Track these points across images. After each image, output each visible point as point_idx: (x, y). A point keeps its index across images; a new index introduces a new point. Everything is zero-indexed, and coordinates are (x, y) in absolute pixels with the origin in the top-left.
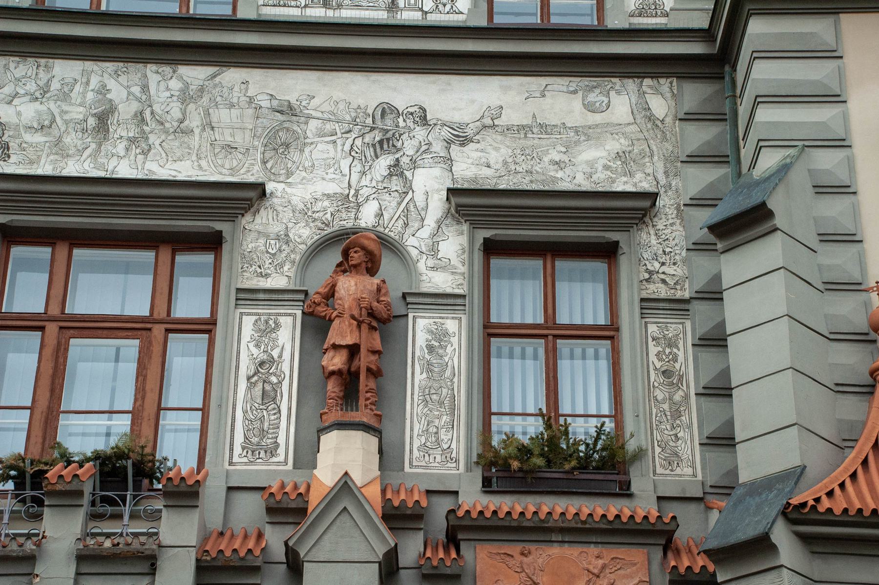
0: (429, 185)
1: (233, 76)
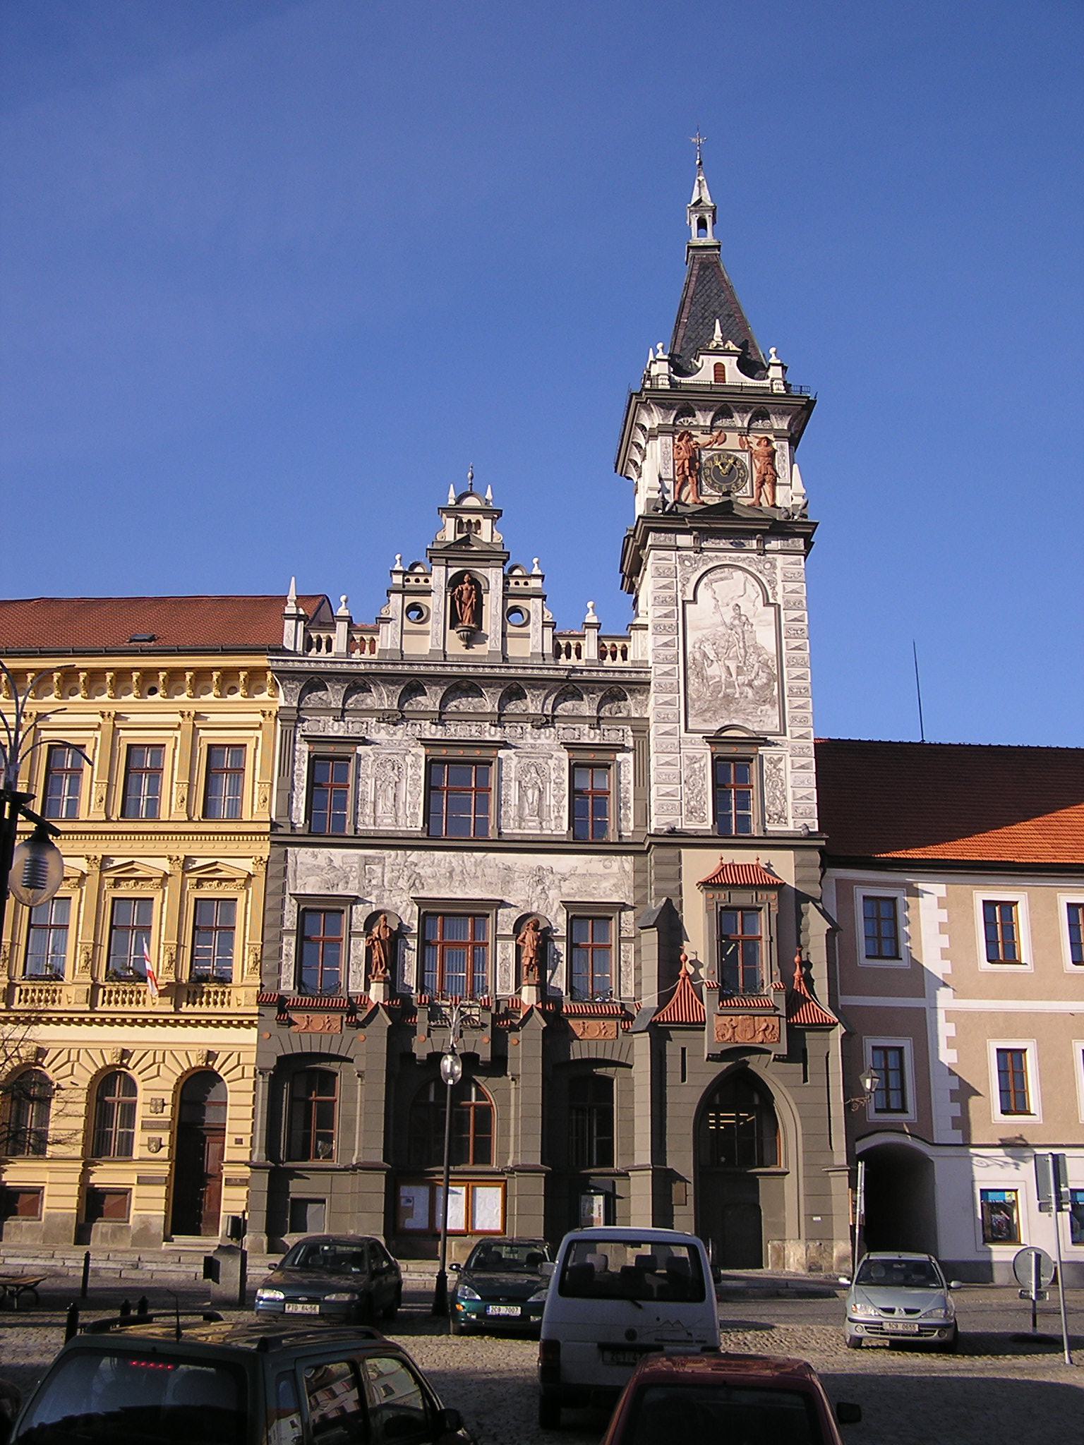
0: (555, 897)
1: (491, 855)
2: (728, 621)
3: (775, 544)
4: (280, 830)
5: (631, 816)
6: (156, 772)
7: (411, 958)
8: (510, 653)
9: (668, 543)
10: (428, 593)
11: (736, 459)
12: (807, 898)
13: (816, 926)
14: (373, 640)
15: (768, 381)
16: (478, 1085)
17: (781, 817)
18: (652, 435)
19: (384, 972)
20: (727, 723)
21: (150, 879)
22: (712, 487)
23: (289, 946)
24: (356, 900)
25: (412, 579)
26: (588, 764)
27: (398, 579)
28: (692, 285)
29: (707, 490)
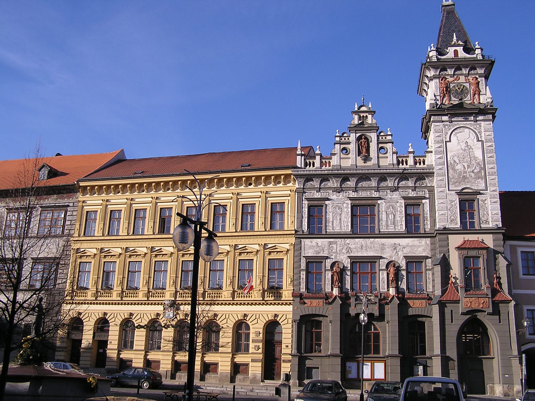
0: (401, 254)
1: (377, 240)
2: (463, 148)
3: (480, 118)
4: (298, 233)
5: (429, 223)
6: (253, 213)
7: (348, 278)
8: (381, 164)
9: (439, 120)
10: (349, 143)
11: (464, 86)
12: (498, 253)
13: (502, 263)
14: (329, 162)
15: (475, 55)
16: (374, 325)
17: (487, 222)
18: (431, 79)
19: (338, 284)
20: (464, 187)
21: (252, 252)
22: (455, 97)
23: (303, 275)
24: (327, 258)
25: (343, 138)
26: (412, 205)
27: (338, 139)
28: (444, 21)
29: (453, 99)
